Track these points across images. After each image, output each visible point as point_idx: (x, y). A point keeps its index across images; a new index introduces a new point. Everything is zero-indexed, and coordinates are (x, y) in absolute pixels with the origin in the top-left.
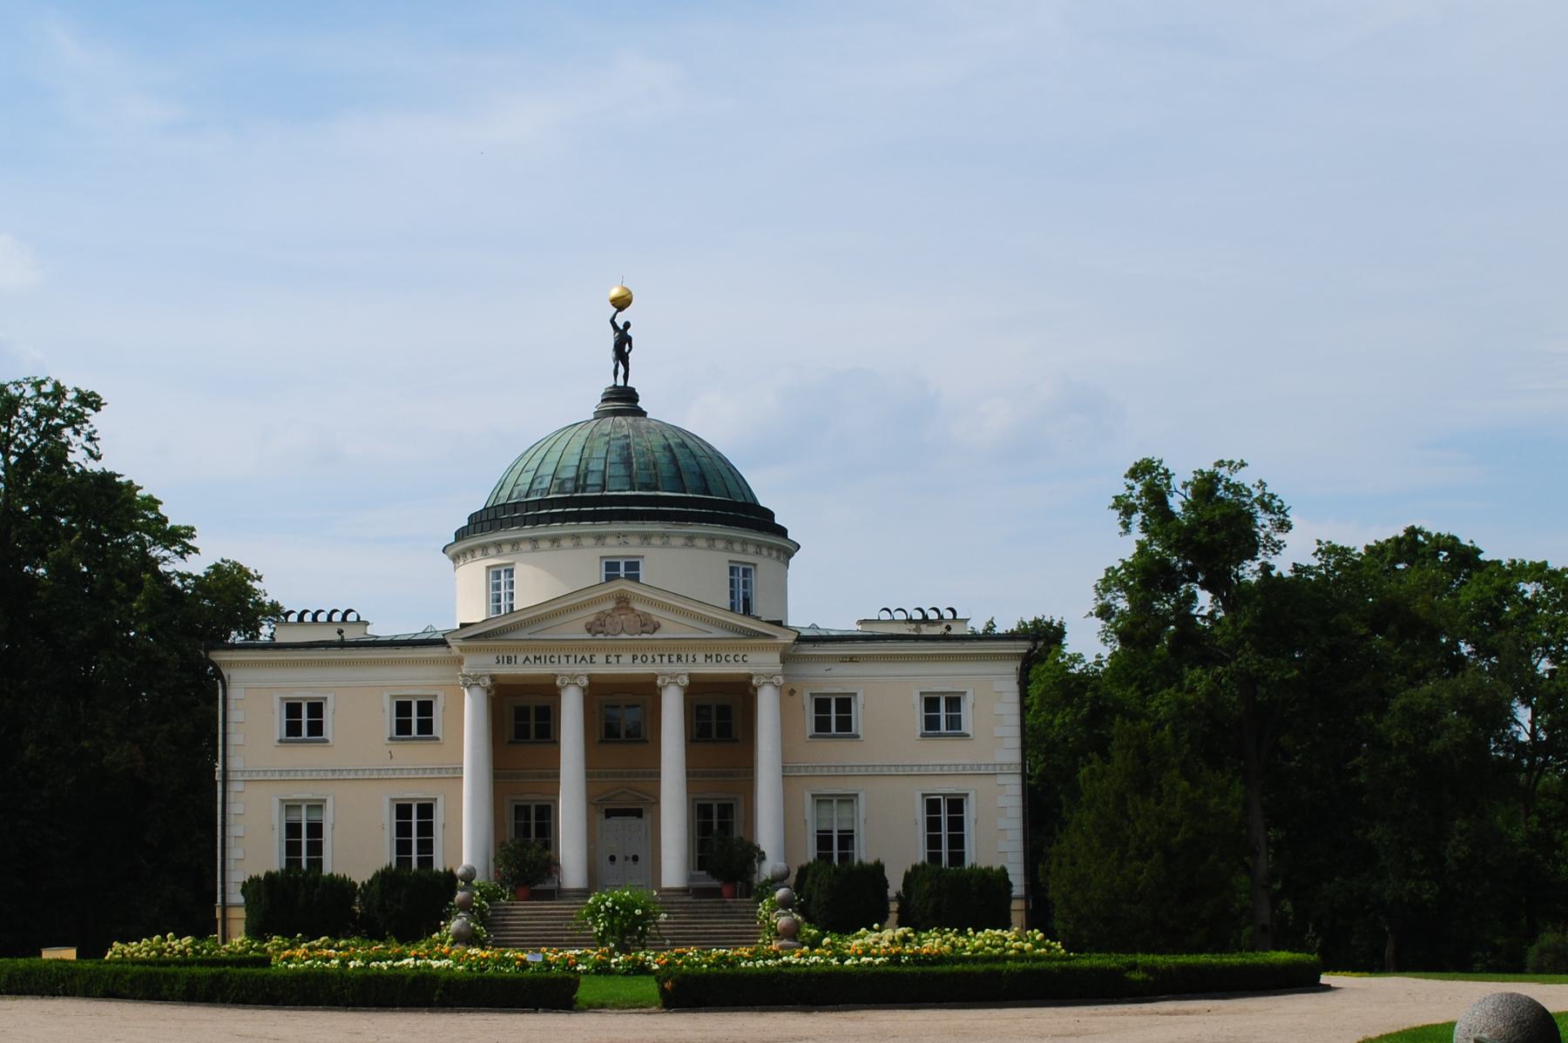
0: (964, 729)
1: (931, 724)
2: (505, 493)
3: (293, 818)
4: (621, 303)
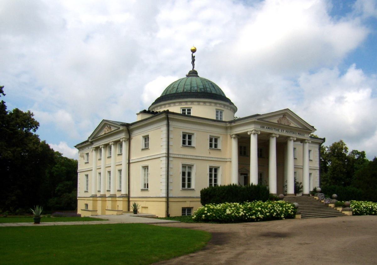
3: (184, 170)
4: (194, 51)
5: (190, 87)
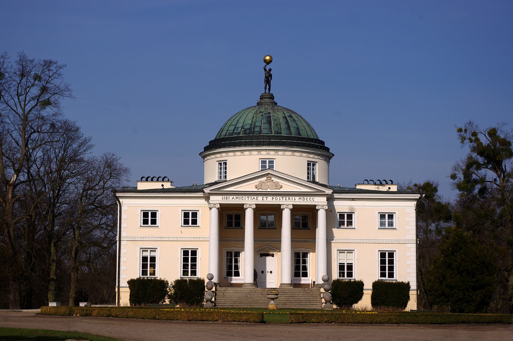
0: (394, 227)
1: (382, 224)
2: (224, 133)
3: (145, 254)
5: (233, 129)
